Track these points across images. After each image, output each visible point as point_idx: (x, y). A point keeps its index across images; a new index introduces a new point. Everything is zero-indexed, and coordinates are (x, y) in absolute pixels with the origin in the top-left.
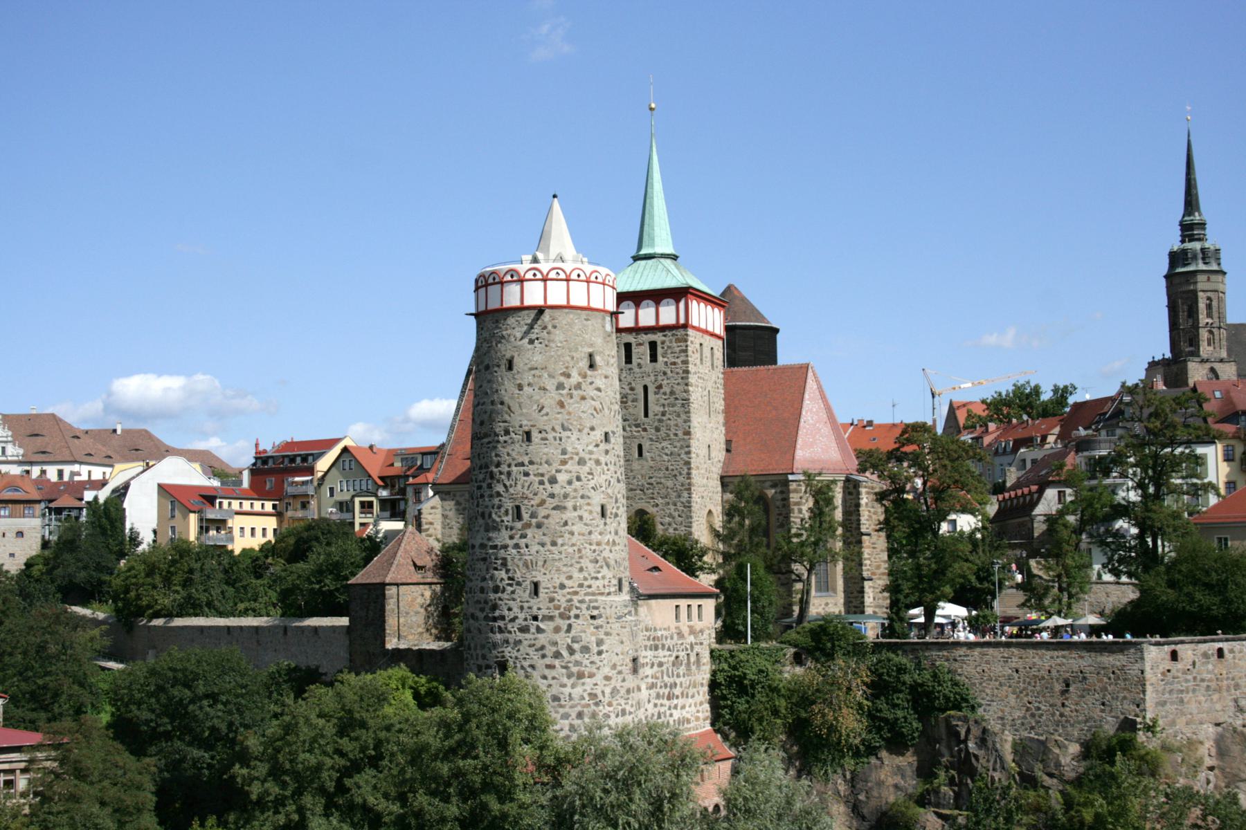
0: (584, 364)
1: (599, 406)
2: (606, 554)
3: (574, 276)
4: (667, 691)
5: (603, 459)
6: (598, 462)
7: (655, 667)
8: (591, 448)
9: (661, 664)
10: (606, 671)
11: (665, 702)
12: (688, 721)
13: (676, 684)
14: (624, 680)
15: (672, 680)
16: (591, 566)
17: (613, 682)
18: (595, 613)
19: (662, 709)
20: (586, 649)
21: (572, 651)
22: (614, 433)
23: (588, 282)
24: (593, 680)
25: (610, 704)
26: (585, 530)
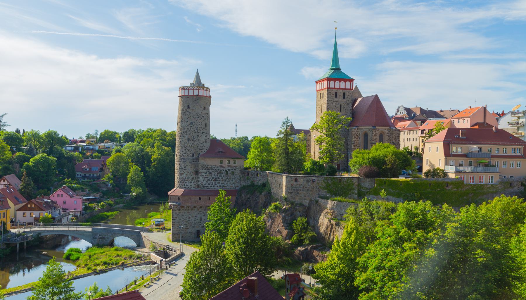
0: (187, 107)
1: (189, 116)
2: (188, 149)
3: (185, 89)
4: (213, 179)
5: (189, 128)
6: (188, 129)
7: (208, 174)
8: (187, 126)
9: (210, 173)
10: (186, 173)
11: (212, 181)
12: (225, 186)
13: (219, 178)
14: (191, 176)
15: (217, 177)
16: (184, 151)
17: (188, 176)
18: (184, 161)
19: (210, 183)
20: (182, 168)
21: (180, 169)
22: (194, 122)
23: (189, 89)
24: (183, 175)
25: (187, 180)
26: (184, 143)
